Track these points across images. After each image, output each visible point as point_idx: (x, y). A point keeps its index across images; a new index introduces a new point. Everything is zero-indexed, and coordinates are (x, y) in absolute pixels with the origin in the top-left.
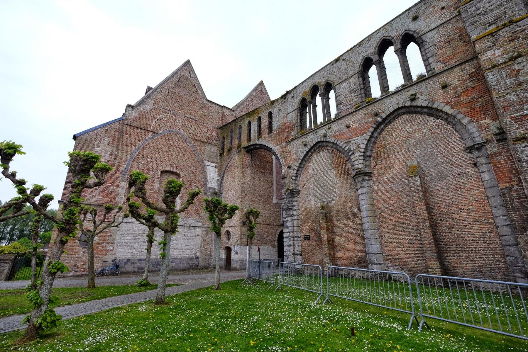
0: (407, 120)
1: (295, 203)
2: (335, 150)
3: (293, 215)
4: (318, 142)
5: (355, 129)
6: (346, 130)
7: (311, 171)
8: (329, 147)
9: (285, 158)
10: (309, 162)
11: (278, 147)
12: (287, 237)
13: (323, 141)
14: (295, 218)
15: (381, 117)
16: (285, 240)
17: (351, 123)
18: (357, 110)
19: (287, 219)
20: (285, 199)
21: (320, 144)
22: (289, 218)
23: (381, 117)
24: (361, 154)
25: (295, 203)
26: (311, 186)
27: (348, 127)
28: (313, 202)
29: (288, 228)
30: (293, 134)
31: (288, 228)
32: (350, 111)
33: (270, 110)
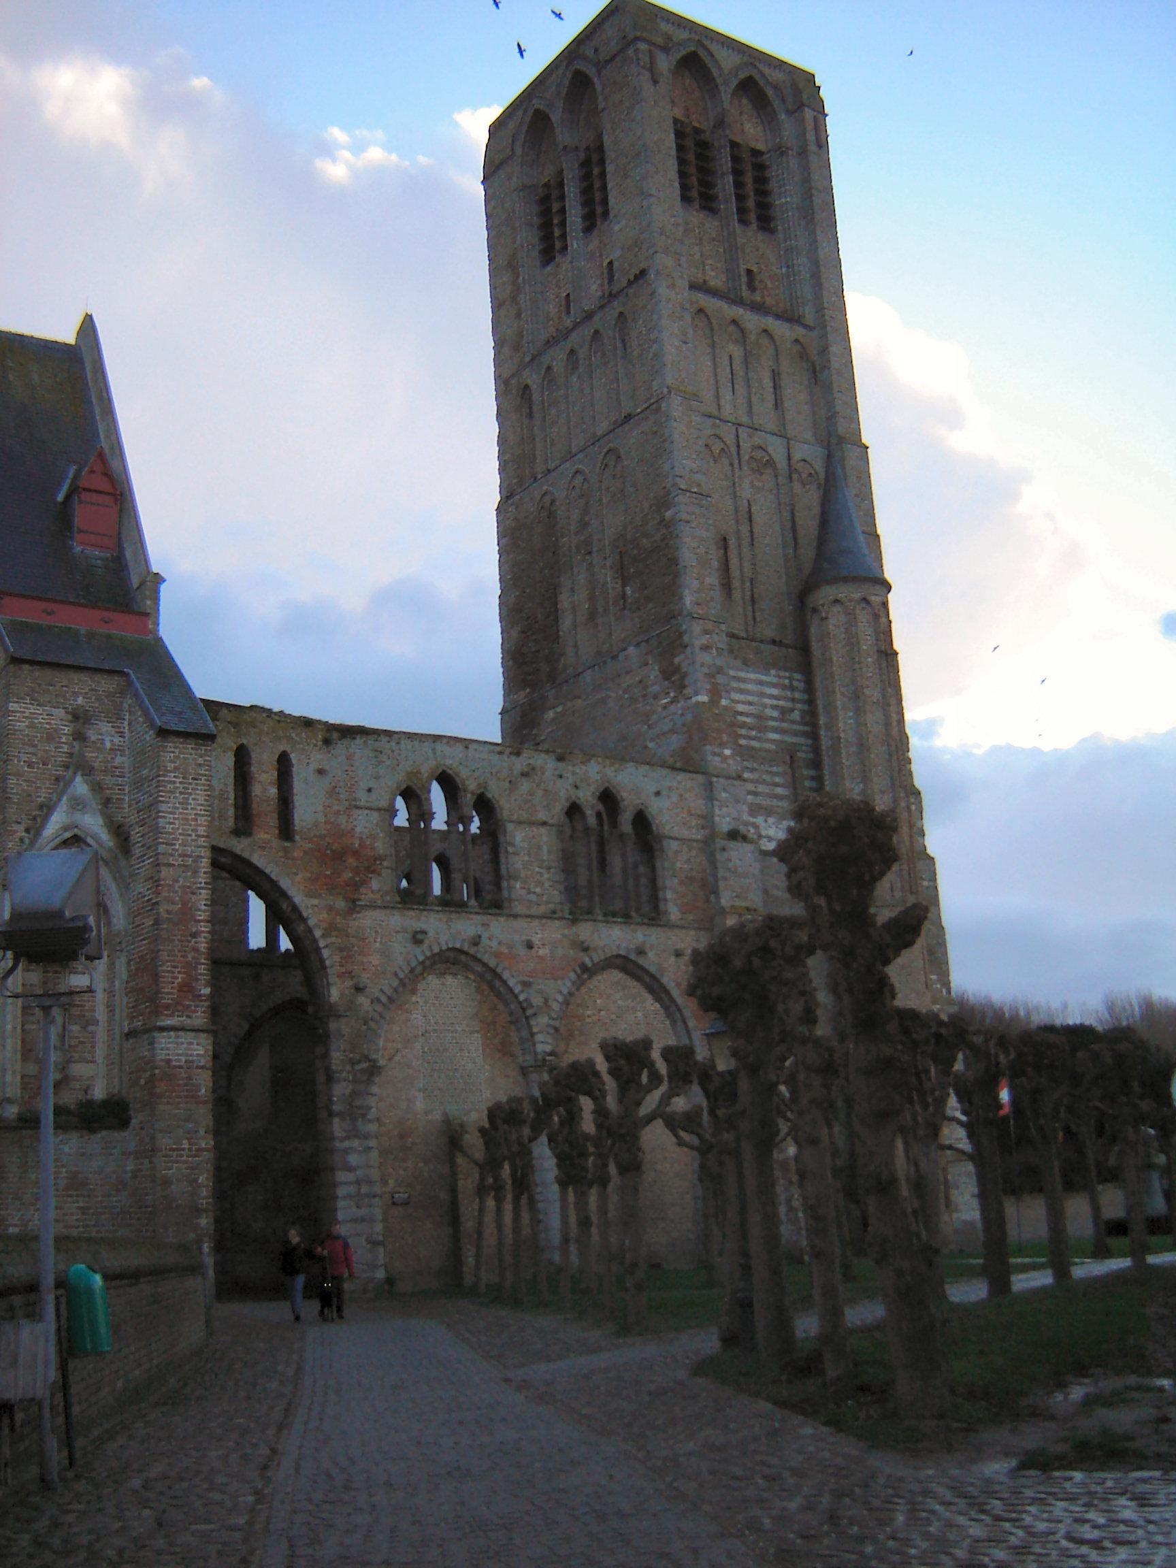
0: (618, 983)
1: (372, 1101)
2: (485, 987)
3: (366, 1136)
4: (454, 949)
5: (541, 958)
6: (522, 951)
7: (417, 1017)
8: (473, 971)
9: (341, 950)
10: (414, 992)
11: (315, 902)
12: (350, 1196)
13: (466, 954)
14: (373, 1143)
15: (591, 958)
16: (341, 1204)
17: (536, 940)
18: (551, 915)
19: (347, 1144)
20: (344, 1084)
21: (452, 955)
22: (356, 1143)
23: (591, 958)
24: (552, 1022)
25: (372, 1101)
26: (416, 1063)
27: (530, 946)
28: (420, 1104)
29: (351, 1169)
30: (375, 884)
31: (351, 1169)
32: (534, 911)
33: (288, 750)
